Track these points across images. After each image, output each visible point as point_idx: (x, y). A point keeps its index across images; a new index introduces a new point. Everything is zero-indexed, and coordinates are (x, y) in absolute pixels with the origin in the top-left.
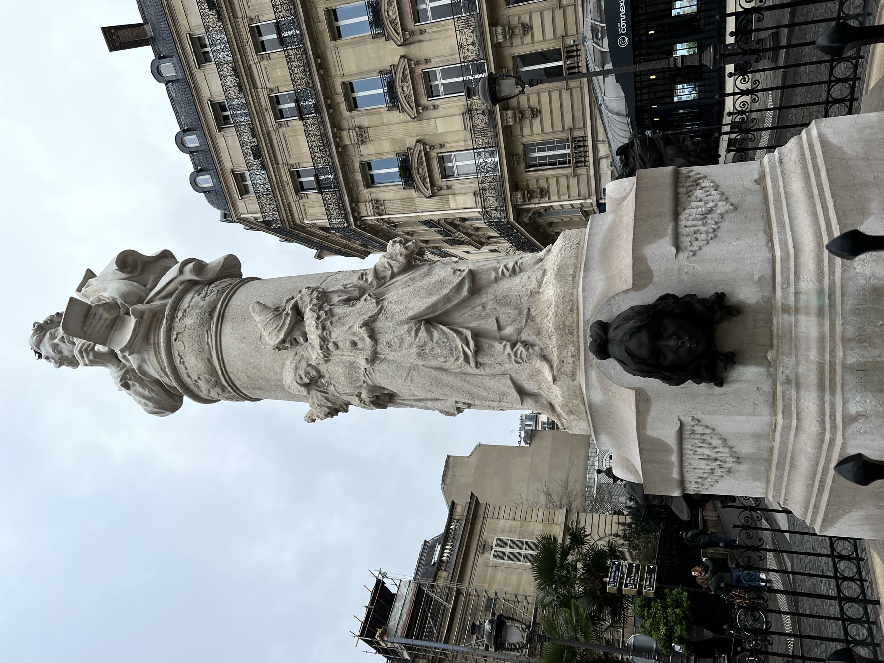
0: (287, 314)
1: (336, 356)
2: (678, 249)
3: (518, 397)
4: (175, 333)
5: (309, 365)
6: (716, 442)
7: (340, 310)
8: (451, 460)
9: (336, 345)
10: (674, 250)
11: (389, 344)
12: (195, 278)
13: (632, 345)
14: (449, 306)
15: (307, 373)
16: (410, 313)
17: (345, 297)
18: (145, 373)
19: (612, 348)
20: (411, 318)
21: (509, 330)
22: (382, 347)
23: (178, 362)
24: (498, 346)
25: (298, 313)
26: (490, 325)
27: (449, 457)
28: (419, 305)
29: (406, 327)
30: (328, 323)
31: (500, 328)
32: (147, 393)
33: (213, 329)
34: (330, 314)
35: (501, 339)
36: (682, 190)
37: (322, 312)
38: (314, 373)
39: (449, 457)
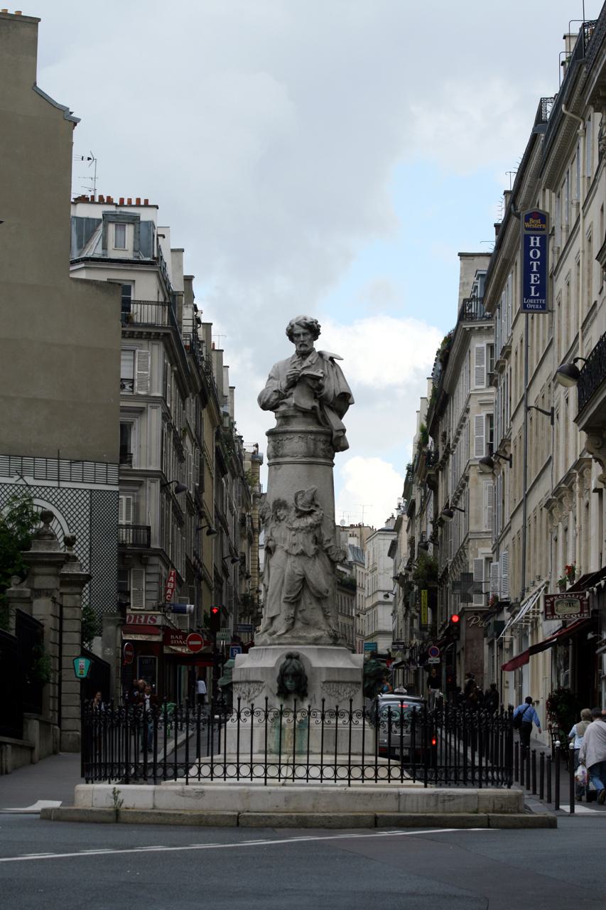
0: (309, 507)
1: (289, 535)
2: (324, 683)
3: (271, 616)
4: (303, 436)
5: (285, 517)
6: (256, 694)
7: (311, 537)
8: (25, 31)
9: (294, 535)
10: (324, 680)
11: (294, 562)
12: (334, 437)
13: (290, 667)
14: (311, 588)
15: (282, 515)
16: (307, 572)
17: (317, 536)
18: (283, 403)
19: (289, 661)
20: (305, 572)
21: (299, 615)
22: (292, 558)
23: (288, 436)
24: (292, 612)
25: (310, 513)
26: (302, 606)
27: (34, 22)
28: (311, 577)
29: (301, 569)
30: (304, 531)
31: (300, 611)
32: (271, 400)
33: (304, 460)
34: (309, 532)
35: (295, 612)
36: (350, 684)
37: (309, 528)
38: (282, 518)
39: (34, 22)
